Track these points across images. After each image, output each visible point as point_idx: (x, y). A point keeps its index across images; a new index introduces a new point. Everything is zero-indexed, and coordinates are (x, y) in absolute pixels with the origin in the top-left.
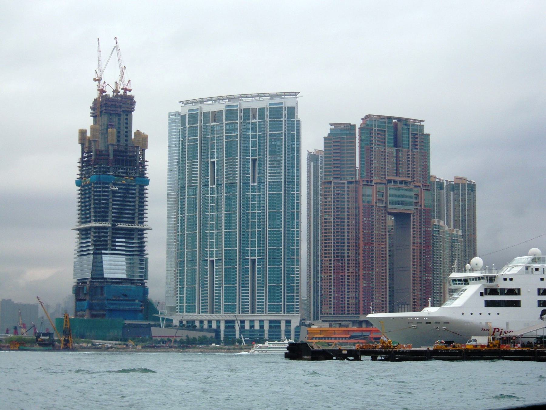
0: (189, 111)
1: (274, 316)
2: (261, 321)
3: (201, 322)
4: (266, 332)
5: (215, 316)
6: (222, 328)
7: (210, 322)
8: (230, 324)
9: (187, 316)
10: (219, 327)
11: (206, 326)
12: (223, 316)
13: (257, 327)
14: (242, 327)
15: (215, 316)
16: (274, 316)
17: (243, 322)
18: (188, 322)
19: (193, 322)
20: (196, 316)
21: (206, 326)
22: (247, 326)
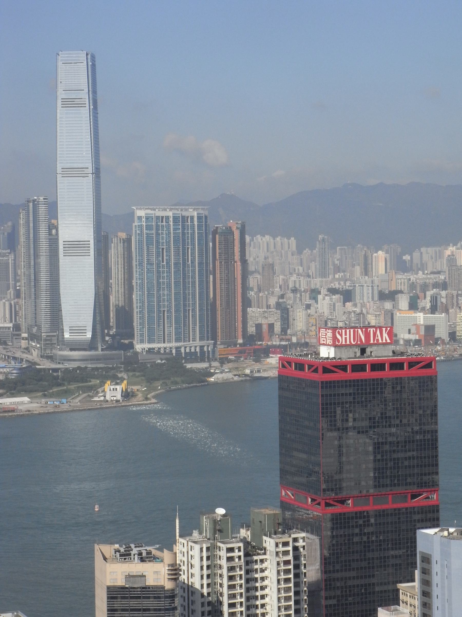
0: (146, 214)
1: (202, 343)
2: (196, 347)
3: (159, 349)
4: (199, 353)
5: (167, 345)
6: (174, 351)
7: (165, 348)
8: (178, 348)
9: (147, 346)
10: (171, 351)
11: (162, 351)
12: (174, 344)
13: (193, 350)
14: (185, 350)
15: (167, 345)
16: (202, 343)
17: (185, 347)
18: (150, 349)
19: (154, 349)
20: (155, 345)
21: (162, 351)
22: (188, 350)
